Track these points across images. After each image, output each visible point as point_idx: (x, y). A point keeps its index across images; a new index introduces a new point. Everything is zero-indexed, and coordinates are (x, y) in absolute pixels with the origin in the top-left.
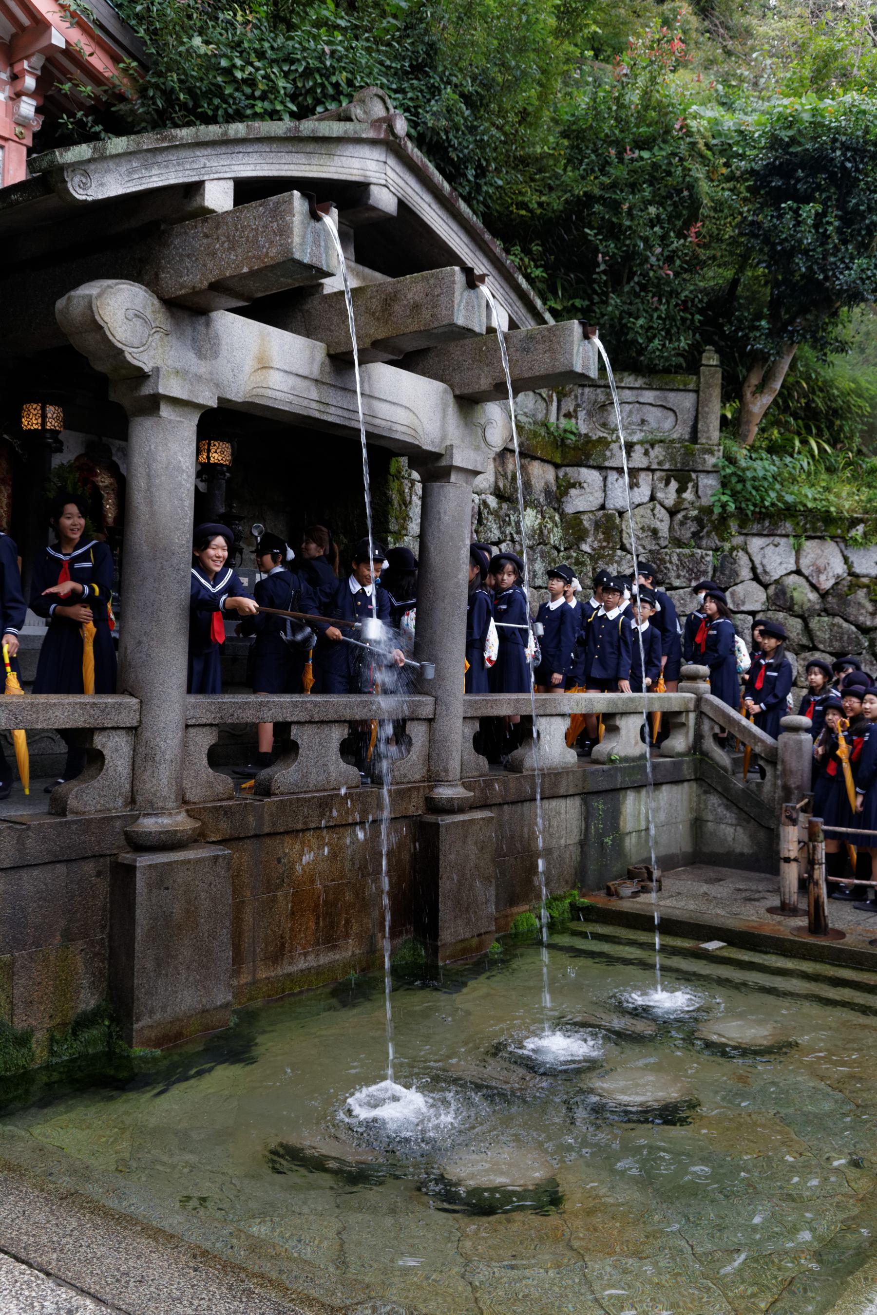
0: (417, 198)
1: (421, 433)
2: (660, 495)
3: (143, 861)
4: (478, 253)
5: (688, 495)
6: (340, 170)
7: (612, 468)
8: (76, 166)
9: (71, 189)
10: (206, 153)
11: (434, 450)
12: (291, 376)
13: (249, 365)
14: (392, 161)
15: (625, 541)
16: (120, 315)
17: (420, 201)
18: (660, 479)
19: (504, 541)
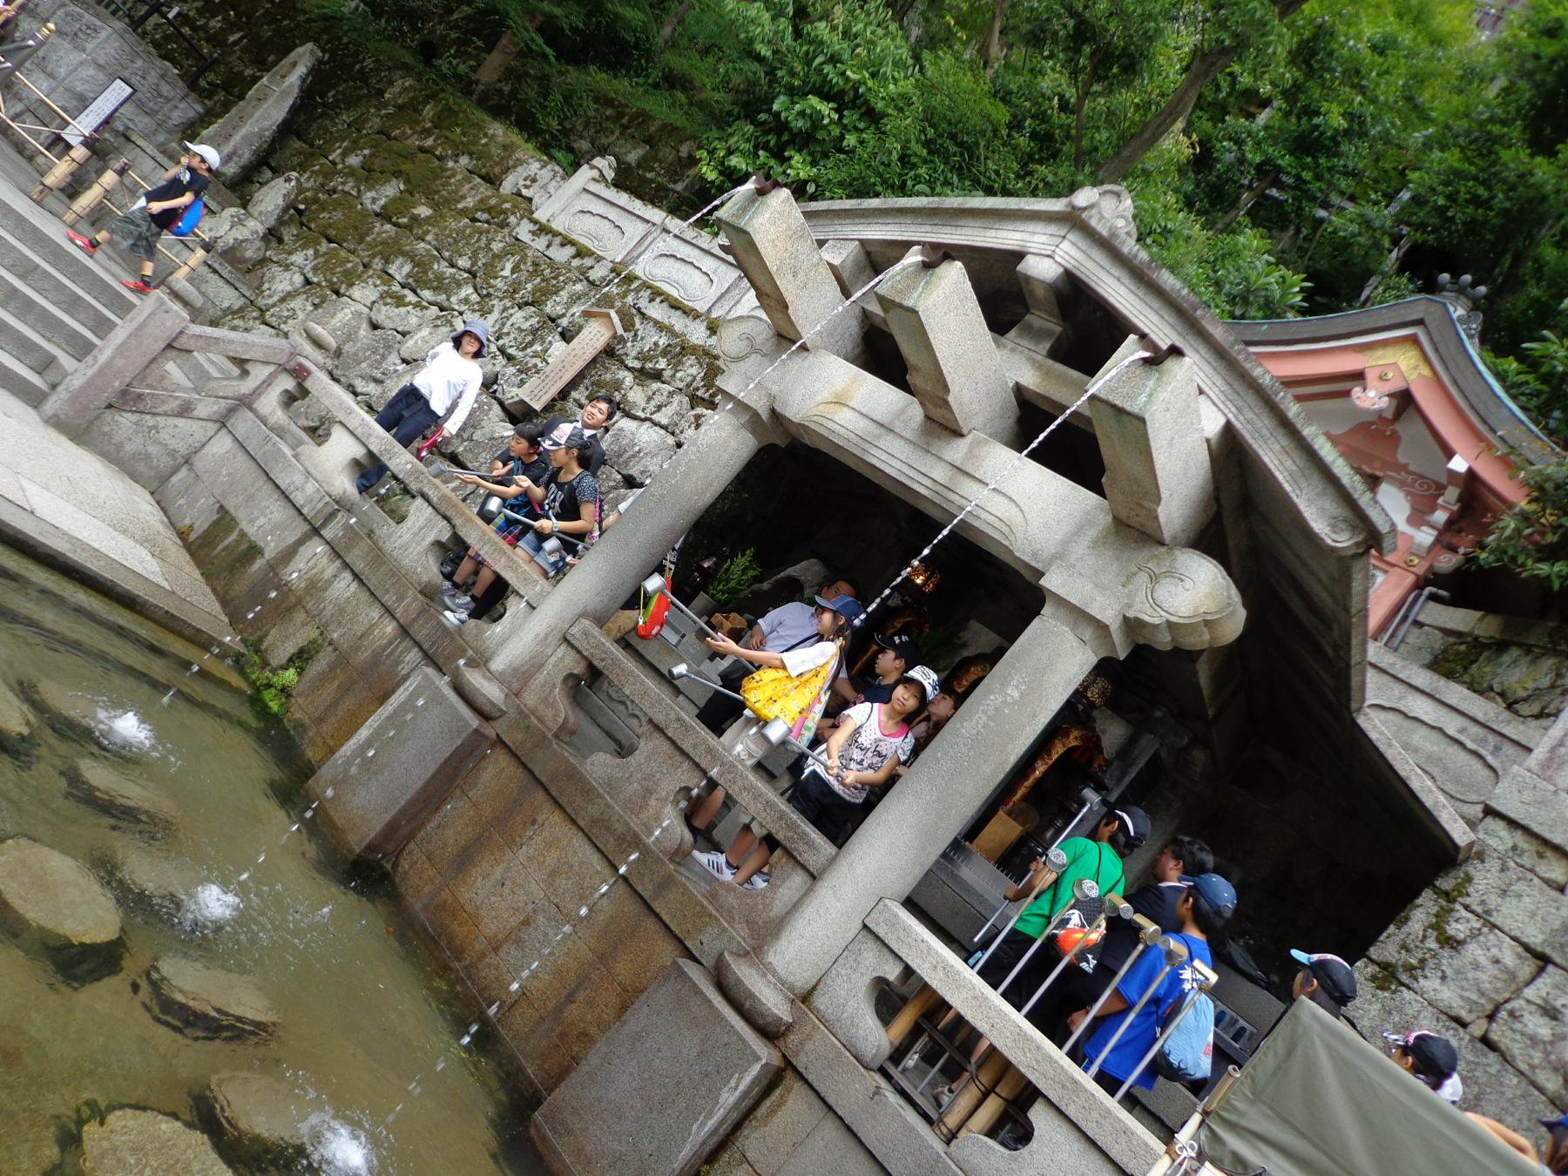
0: (1099, 272)
4: (1189, 337)
11: (1033, 564)
13: (826, 394)
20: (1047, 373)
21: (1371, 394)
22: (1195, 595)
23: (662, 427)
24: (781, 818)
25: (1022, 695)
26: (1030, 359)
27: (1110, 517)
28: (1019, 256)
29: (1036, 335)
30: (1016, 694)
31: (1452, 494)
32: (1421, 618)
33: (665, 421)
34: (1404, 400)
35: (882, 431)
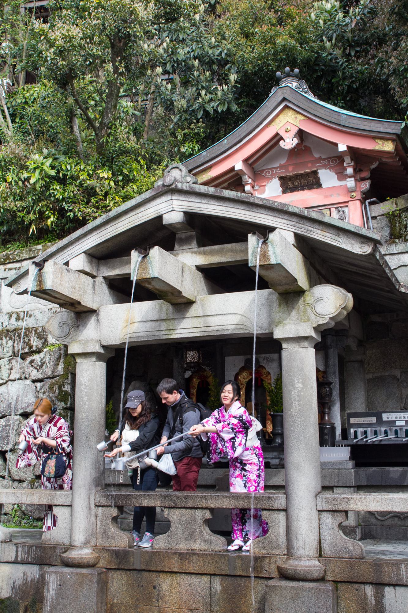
11: (264, 332)
12: (148, 323)
20: (205, 253)
21: (287, 140)
22: (330, 301)
23: (19, 379)
25: (303, 384)
26: (192, 252)
27: (277, 295)
28: (159, 218)
29: (186, 241)
30: (300, 385)
31: (347, 160)
32: (373, 215)
33: (18, 376)
34: (301, 134)
35: (159, 322)
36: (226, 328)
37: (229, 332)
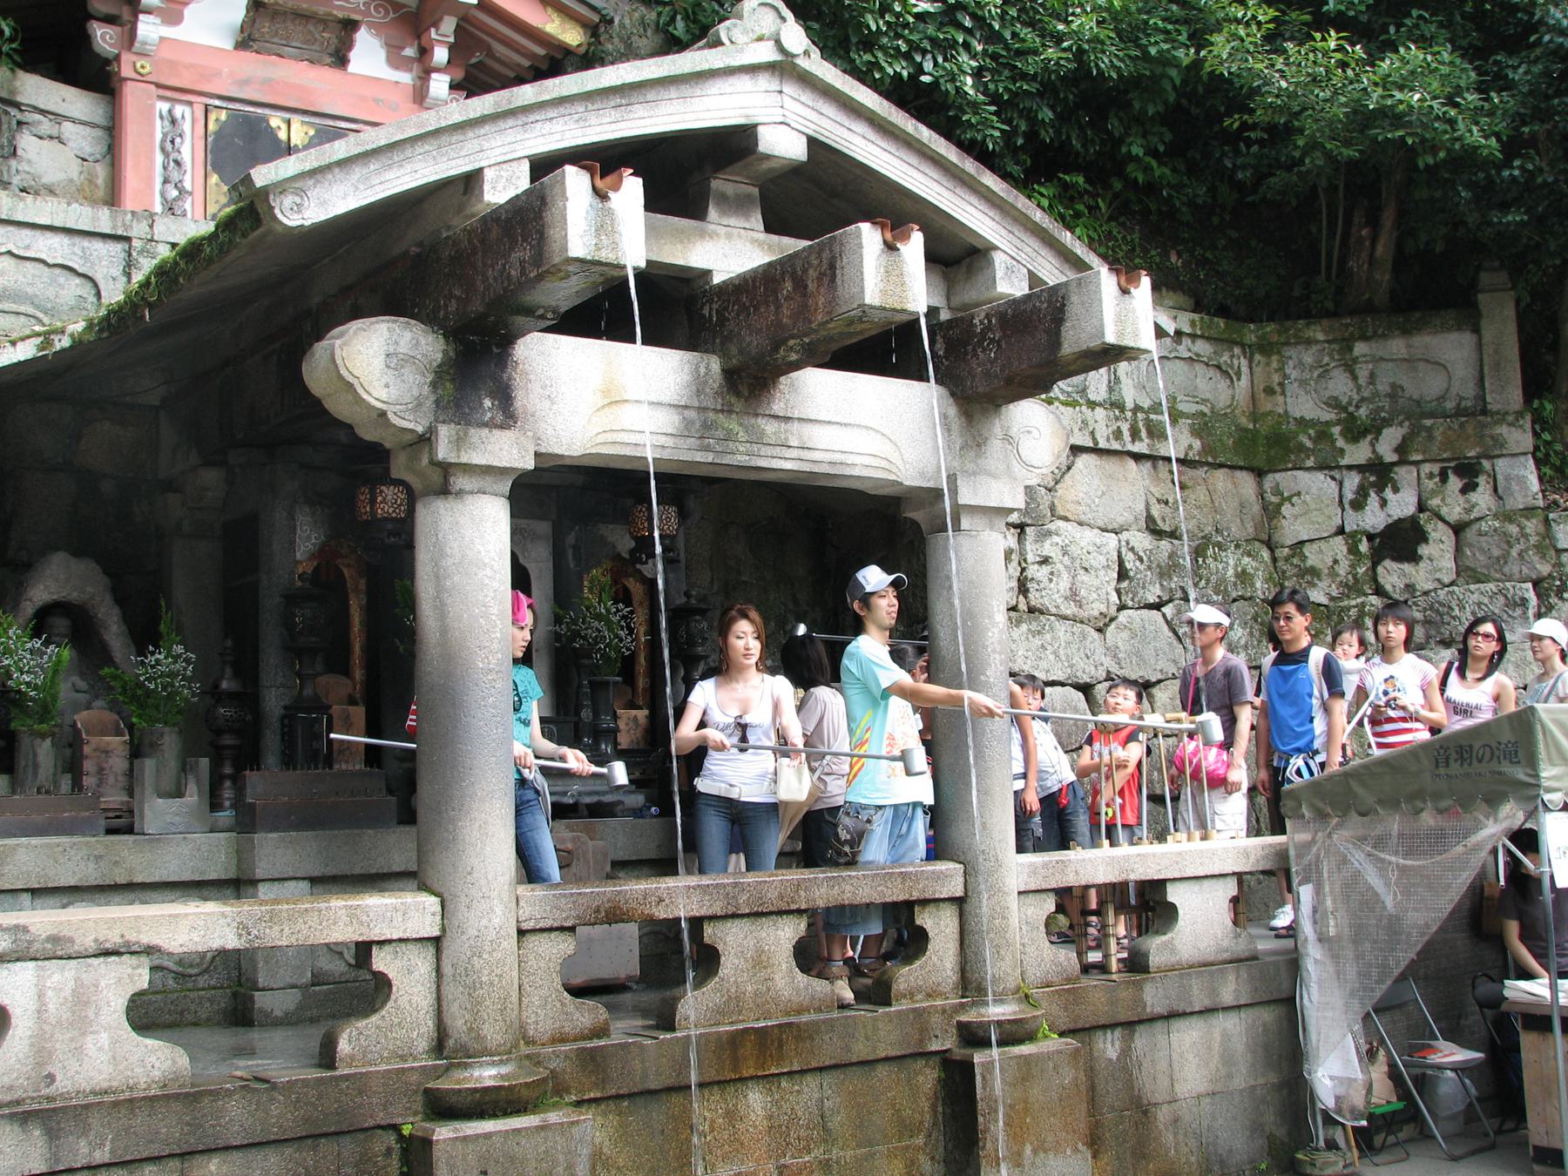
1: (899, 463)
2: (1434, 502)
3: (444, 1132)
4: (958, 190)
5: (1482, 498)
6: (701, 115)
7: (1350, 468)
8: (282, 187)
9: (280, 216)
10: (482, 131)
11: (925, 485)
14: (790, 89)
15: (1380, 580)
16: (378, 362)
17: (846, 134)
18: (1431, 476)
19: (1170, 601)
24: (904, 880)
36: (850, 459)
37: (856, 472)
